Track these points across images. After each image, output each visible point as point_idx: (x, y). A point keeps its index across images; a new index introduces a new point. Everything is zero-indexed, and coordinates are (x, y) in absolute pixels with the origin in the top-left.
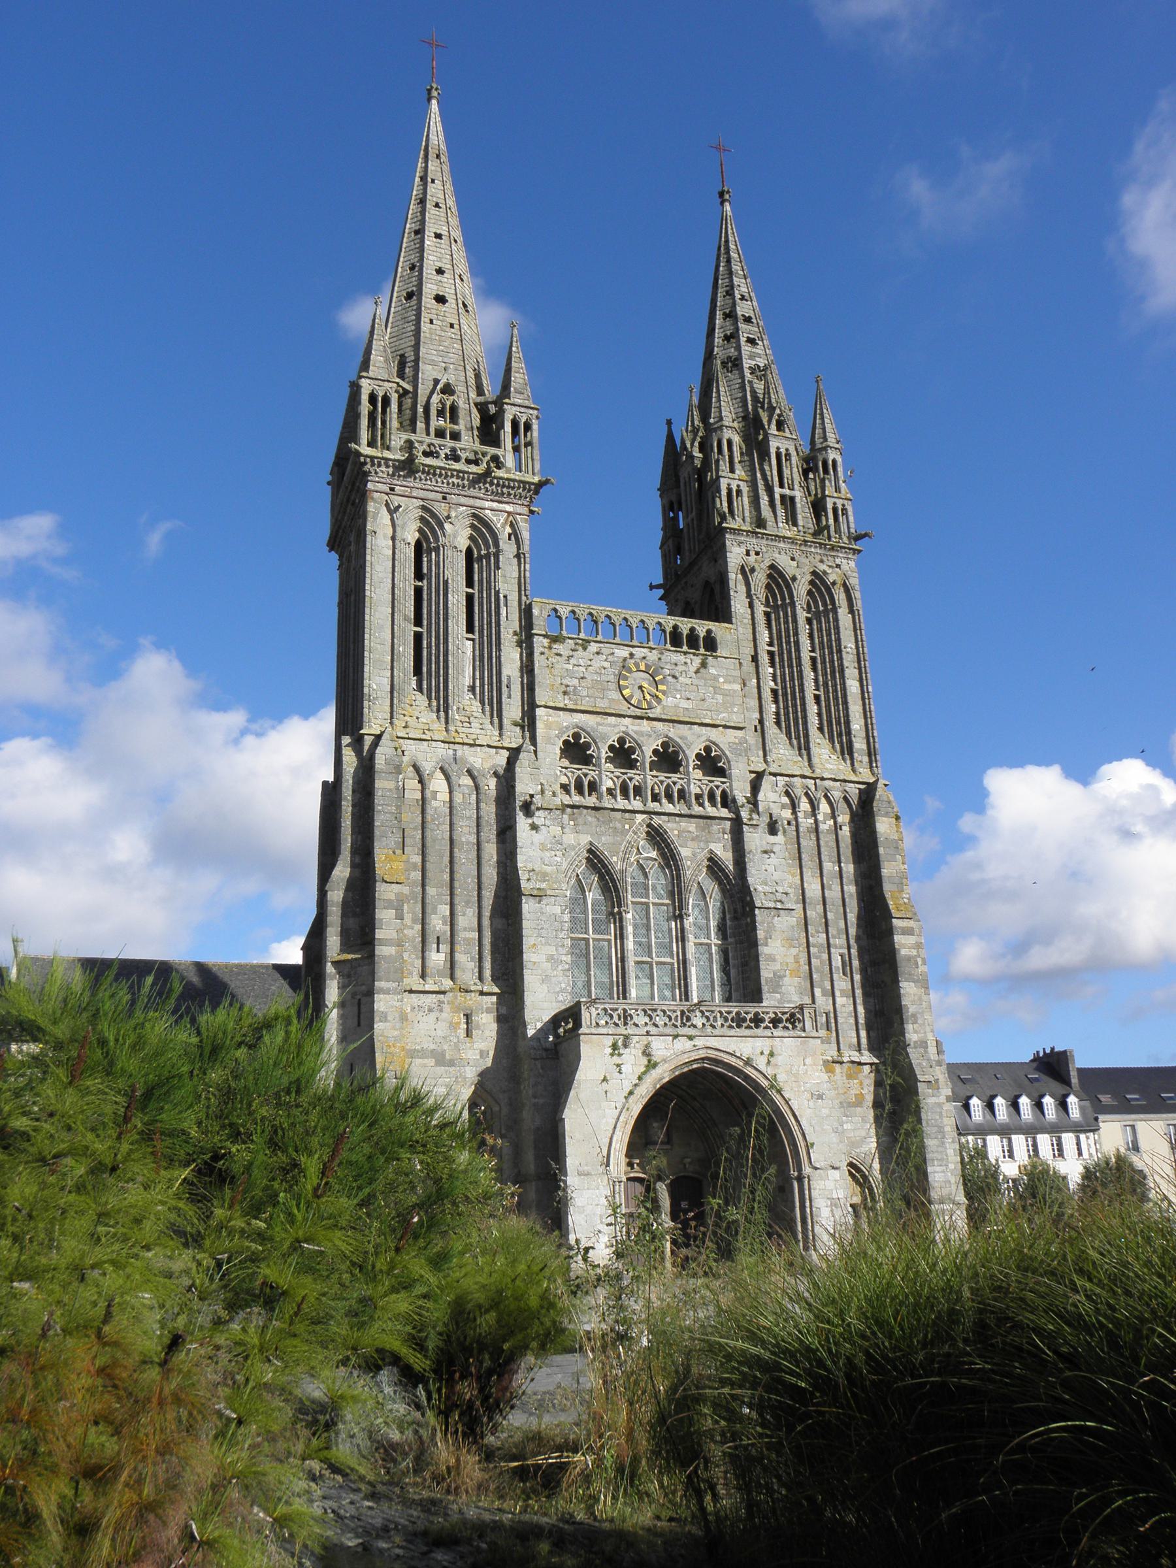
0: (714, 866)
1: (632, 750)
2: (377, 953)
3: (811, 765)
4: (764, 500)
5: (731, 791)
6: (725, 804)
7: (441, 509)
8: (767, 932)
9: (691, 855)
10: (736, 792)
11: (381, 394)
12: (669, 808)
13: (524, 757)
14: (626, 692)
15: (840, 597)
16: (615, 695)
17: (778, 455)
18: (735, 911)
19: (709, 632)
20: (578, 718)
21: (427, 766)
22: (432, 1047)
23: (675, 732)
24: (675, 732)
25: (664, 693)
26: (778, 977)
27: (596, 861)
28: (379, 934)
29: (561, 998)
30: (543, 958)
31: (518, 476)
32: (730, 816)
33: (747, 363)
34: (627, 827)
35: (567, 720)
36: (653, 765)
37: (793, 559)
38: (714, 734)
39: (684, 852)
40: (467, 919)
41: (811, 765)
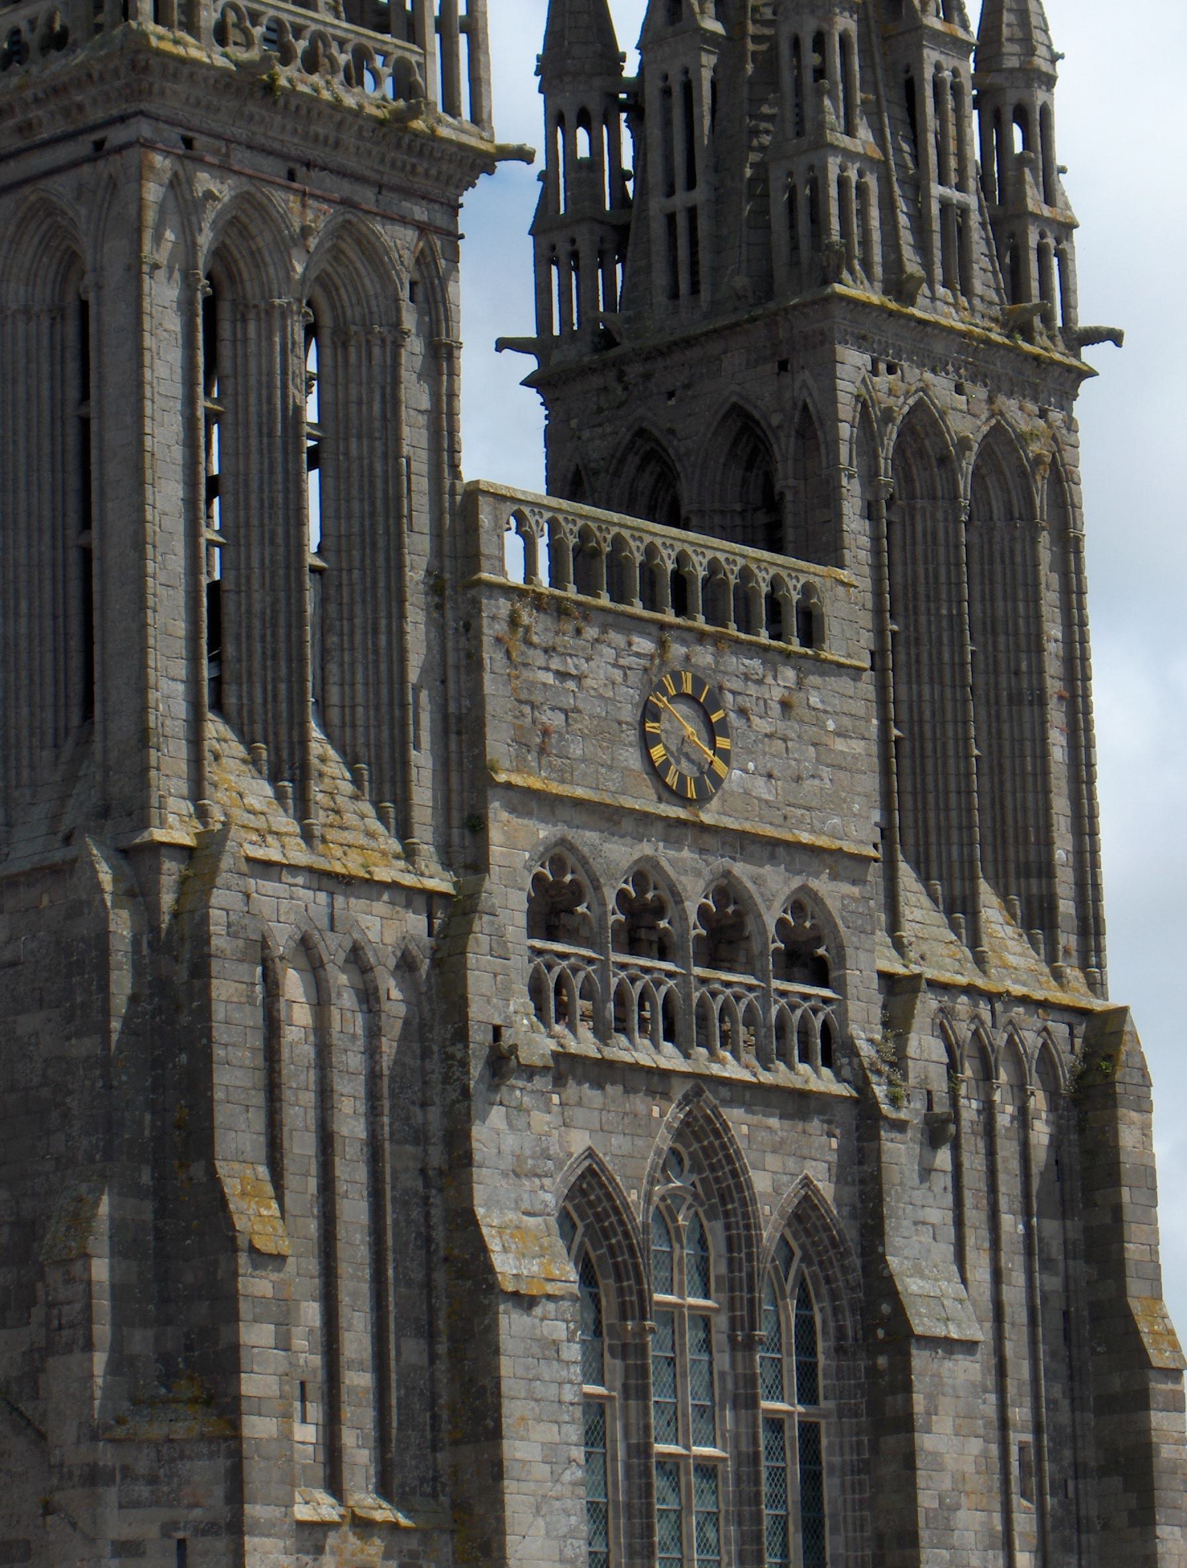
2: (246, 1432)
3: (980, 961)
5: (844, 1022)
8: (931, 1397)
10: (855, 1030)
14: (657, 752)
16: (631, 758)
18: (841, 1334)
19: (808, 590)
25: (725, 756)
26: (948, 1508)
29: (569, 1553)
32: (843, 1090)
34: (656, 1111)
37: (959, 389)
39: (761, 1182)
41: (980, 961)
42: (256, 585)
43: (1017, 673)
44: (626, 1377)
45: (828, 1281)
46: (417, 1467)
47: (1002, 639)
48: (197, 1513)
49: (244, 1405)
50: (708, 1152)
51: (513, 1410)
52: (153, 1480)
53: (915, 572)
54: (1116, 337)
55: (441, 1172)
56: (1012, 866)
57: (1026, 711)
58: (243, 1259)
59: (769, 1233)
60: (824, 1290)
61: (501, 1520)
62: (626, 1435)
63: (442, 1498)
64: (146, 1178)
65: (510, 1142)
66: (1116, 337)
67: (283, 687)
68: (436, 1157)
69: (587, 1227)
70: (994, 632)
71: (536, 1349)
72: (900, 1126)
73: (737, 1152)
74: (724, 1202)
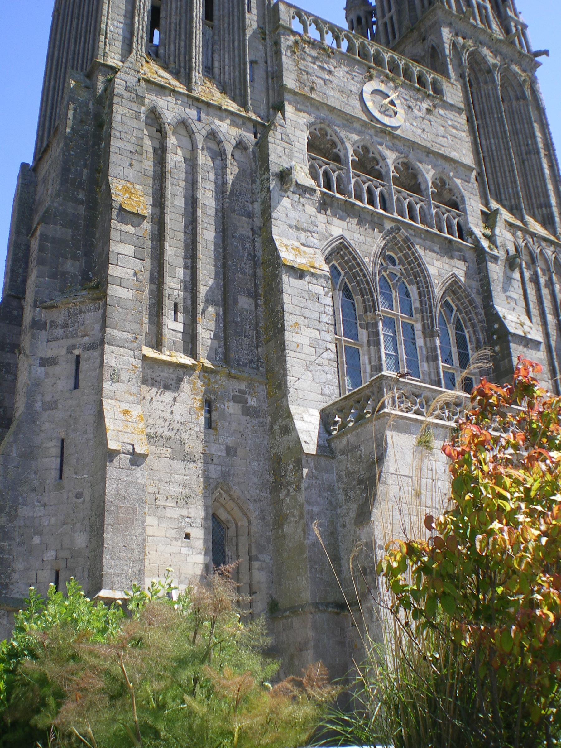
2: (109, 292)
5: (467, 222)
18: (478, 340)
22: (167, 434)
28: (113, 271)
29: (327, 391)
30: (306, 341)
42: (173, 13)
43: (528, 145)
44: (369, 337)
45: (470, 320)
46: (247, 355)
47: (520, 136)
48: (86, 339)
49: (110, 279)
50: (406, 256)
51: (289, 320)
52: (65, 326)
53: (483, 107)
54: (546, 53)
55: (260, 229)
56: (535, 205)
57: (533, 157)
58: (115, 213)
59: (438, 292)
60: (469, 324)
61: (285, 370)
62: (370, 363)
63: (261, 369)
64: (81, 195)
65: (293, 214)
66: (546, 53)
67: (182, 43)
68: (258, 222)
69: (345, 273)
70: (517, 134)
71: (305, 295)
72: (495, 259)
73: (419, 255)
74: (416, 279)
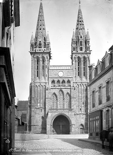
0: (68, 93)
1: (59, 81)
4: (78, 48)
6: (70, 86)
7: (39, 56)
9: (65, 93)
11: (32, 44)
12: (63, 87)
13: (47, 84)
15: (87, 59)
17: (80, 41)
20: (53, 79)
21: (37, 86)
23: (64, 79)
24: (64, 79)
27: (54, 94)
31: (47, 51)
33: (79, 29)
35: (52, 79)
36: (62, 83)
38: (69, 79)
40: (42, 101)
